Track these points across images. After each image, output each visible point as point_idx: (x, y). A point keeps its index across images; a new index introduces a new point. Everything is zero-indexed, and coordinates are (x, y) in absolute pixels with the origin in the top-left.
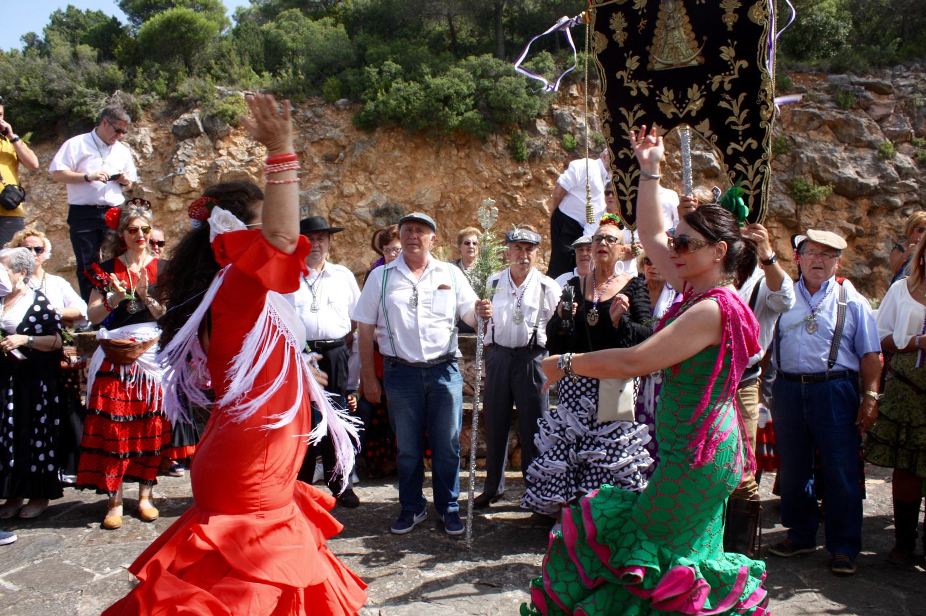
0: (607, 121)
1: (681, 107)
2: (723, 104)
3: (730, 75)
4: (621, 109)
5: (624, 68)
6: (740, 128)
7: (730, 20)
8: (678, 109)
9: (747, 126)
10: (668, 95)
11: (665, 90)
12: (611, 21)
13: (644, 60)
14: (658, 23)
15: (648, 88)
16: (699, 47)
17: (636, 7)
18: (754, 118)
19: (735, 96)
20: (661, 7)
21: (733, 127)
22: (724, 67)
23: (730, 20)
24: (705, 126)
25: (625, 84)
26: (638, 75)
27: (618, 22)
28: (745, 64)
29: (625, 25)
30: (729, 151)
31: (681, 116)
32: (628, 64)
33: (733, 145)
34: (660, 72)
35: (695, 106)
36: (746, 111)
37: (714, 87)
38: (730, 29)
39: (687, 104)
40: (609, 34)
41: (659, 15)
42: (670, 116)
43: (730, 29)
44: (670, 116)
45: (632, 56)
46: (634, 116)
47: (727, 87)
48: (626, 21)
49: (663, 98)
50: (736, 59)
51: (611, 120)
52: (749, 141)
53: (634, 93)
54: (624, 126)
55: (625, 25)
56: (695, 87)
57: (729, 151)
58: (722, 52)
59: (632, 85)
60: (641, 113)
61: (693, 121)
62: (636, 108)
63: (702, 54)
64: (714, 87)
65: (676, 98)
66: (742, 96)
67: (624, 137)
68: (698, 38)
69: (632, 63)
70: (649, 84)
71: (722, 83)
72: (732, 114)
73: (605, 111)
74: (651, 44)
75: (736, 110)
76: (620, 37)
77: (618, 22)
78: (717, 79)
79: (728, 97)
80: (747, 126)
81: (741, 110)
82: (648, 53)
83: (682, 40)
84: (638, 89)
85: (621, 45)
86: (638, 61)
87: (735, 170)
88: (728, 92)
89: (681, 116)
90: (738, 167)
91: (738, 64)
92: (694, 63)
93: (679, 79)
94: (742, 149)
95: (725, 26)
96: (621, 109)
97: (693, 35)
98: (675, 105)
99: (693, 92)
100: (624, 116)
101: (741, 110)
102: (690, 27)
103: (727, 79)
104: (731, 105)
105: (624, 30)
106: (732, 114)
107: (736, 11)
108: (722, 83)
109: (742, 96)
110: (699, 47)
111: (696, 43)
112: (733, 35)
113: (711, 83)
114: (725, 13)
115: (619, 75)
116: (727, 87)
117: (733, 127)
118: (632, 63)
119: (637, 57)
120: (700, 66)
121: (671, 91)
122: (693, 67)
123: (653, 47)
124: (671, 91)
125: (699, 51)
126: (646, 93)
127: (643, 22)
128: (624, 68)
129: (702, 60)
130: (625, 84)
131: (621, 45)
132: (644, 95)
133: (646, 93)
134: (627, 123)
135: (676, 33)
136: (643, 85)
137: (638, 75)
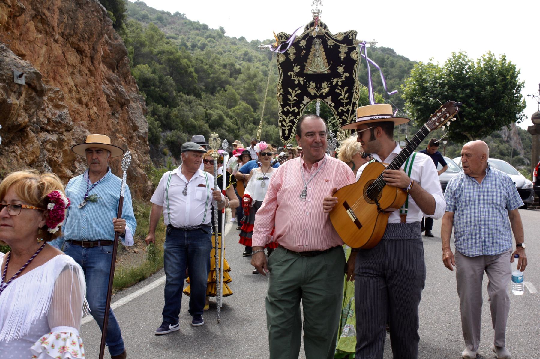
0: (281, 94)
1: (318, 91)
2: (337, 91)
5: (293, 71)
6: (345, 101)
7: (343, 56)
9: (348, 101)
10: (313, 85)
11: (311, 82)
13: (303, 68)
14: (311, 53)
15: (303, 81)
18: (350, 97)
19: (343, 88)
20: (313, 46)
22: (339, 75)
23: (343, 56)
24: (329, 100)
25: (292, 78)
26: (298, 74)
27: (291, 50)
28: (348, 75)
29: (295, 52)
31: (318, 95)
32: (295, 69)
33: (341, 108)
34: (310, 75)
35: (326, 90)
36: (347, 94)
37: (334, 83)
38: (342, 60)
41: (312, 50)
42: (313, 94)
43: (342, 60)
45: (297, 66)
47: (340, 84)
49: (310, 86)
50: (344, 72)
51: (283, 94)
53: (296, 82)
54: (289, 97)
55: (295, 52)
56: (326, 83)
59: (296, 79)
60: (299, 92)
61: (322, 97)
62: (296, 89)
63: (330, 69)
64: (334, 83)
66: (346, 88)
67: (289, 102)
68: (328, 62)
69: (297, 69)
71: (337, 82)
72: (341, 95)
74: (307, 62)
75: (343, 94)
76: (292, 57)
78: (335, 80)
79: (340, 88)
80: (348, 101)
81: (345, 94)
82: (305, 66)
84: (299, 81)
88: (340, 86)
89: (318, 95)
91: (345, 74)
92: (326, 72)
93: (318, 78)
94: (345, 110)
95: (340, 58)
97: (326, 61)
99: (325, 85)
101: (345, 94)
102: (325, 57)
103: (340, 80)
105: (294, 54)
106: (341, 95)
107: (345, 53)
108: (337, 82)
109: (346, 88)
111: (327, 64)
112: (343, 62)
113: (333, 82)
115: (289, 74)
116: (340, 84)
118: (297, 69)
119: (299, 67)
120: (328, 74)
122: (325, 74)
123: (307, 64)
125: (328, 68)
126: (302, 83)
127: (304, 52)
128: (293, 71)
129: (329, 71)
130: (292, 78)
133: (302, 83)
134: (291, 95)
135: (319, 58)
136: (301, 79)
137: (298, 74)
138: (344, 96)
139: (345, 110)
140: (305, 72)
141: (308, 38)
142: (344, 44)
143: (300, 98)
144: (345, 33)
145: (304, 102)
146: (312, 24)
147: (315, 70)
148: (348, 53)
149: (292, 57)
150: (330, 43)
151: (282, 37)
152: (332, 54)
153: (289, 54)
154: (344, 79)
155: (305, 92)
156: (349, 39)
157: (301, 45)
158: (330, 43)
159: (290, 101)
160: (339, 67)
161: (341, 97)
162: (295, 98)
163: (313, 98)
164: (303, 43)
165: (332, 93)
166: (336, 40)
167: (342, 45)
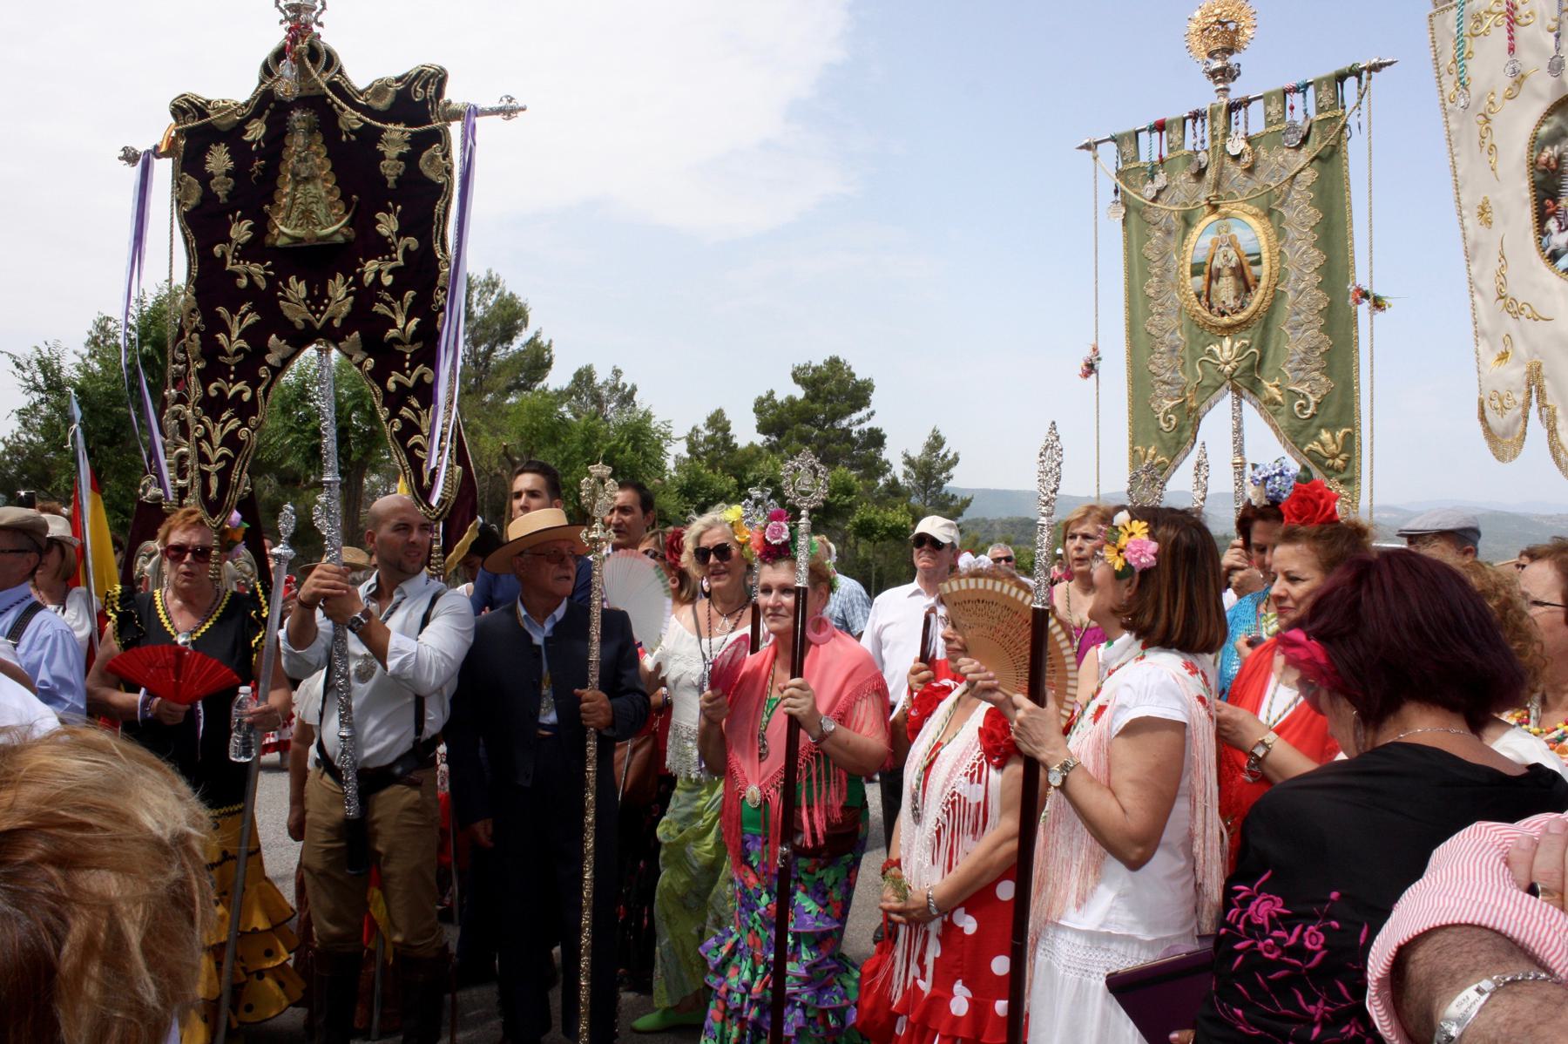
1: (317, 311)
2: (379, 308)
3: (392, 260)
4: (220, 309)
5: (229, 240)
7: (391, 169)
8: (314, 313)
9: (418, 345)
10: (298, 288)
11: (292, 279)
12: (209, 158)
13: (262, 227)
15: (266, 276)
16: (347, 212)
17: (247, 138)
20: (287, 142)
21: (399, 348)
22: (381, 248)
23: (391, 169)
26: (249, 252)
27: (219, 160)
28: (413, 242)
30: (391, 386)
32: (232, 234)
34: (284, 250)
36: (415, 321)
37: (369, 278)
39: (326, 306)
40: (205, 179)
42: (300, 325)
44: (300, 325)
45: (240, 220)
46: (241, 322)
47: (387, 280)
48: (232, 159)
51: (203, 328)
52: (420, 368)
53: (243, 282)
54: (221, 337)
55: (230, 165)
56: (339, 276)
57: (391, 386)
58: (378, 222)
59: (239, 267)
60: (251, 319)
61: (332, 335)
62: (244, 308)
63: (350, 224)
64: (369, 278)
65: (310, 295)
66: (410, 294)
68: (345, 197)
69: (241, 231)
70: (266, 269)
71: (378, 273)
73: (194, 311)
74: (272, 202)
76: (221, 189)
77: (219, 160)
78: (371, 266)
79: (387, 297)
80: (418, 345)
81: (408, 320)
82: (267, 217)
83: (319, 199)
84: (249, 276)
85: (223, 200)
86: (250, 228)
87: (401, 417)
88: (387, 289)
89: (318, 325)
90: (405, 412)
91: (403, 242)
92: (339, 239)
93: (316, 261)
94: (410, 383)
95: (384, 180)
96: (220, 309)
98: (308, 307)
100: (224, 322)
101: (408, 320)
104: (393, 310)
105: (228, 173)
106: (394, 325)
107: (401, 157)
109: (410, 294)
110: (347, 212)
111: (342, 205)
113: (363, 273)
114: (384, 158)
115: (217, 250)
116: (387, 280)
117: (399, 348)
118: (241, 231)
119: (250, 223)
120: (348, 243)
121: (303, 283)
122: (338, 245)
124: (303, 283)
126: (263, 285)
129: (351, 233)
130: (229, 267)
131: (223, 200)
132: (258, 288)
133: (263, 285)
134: (229, 335)
136: (256, 269)
137: (249, 252)
138: (404, 325)
139: (410, 383)
140: (269, 241)
142: (397, 122)
143: (255, 336)
144: (398, 80)
145: (272, 359)
146: (279, 55)
147: (299, 232)
148: (410, 159)
149: (221, 189)
150: (351, 119)
151: (184, 112)
152: (354, 163)
153: (212, 176)
154: (401, 262)
155: (272, 320)
156: (417, 101)
157: (247, 138)
158: (351, 119)
159: (227, 355)
160: (379, 216)
161: (392, 332)
162: (243, 344)
163: (299, 339)
164: (256, 131)
166: (366, 110)
167: (391, 126)
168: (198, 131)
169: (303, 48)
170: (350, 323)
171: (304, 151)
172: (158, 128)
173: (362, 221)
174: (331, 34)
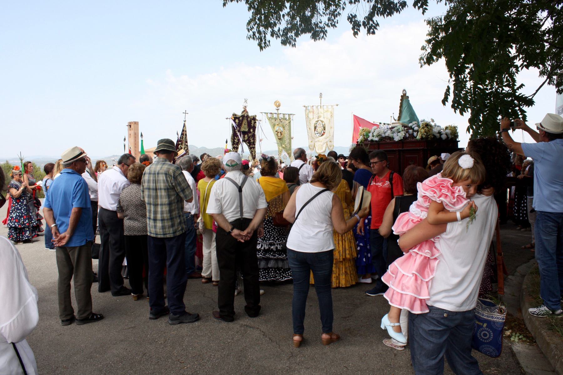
7: (252, 125)
13: (240, 128)
22: (251, 133)
27: (237, 121)
35: (246, 138)
99: (246, 136)
141: (243, 116)
150: (249, 119)
152: (249, 123)
156: (254, 119)
164: (241, 118)
165: (249, 139)
168: (235, 118)
169: (245, 111)
170: (247, 140)
171: (245, 122)
172: (231, 116)
173: (249, 130)
174: (248, 109)
